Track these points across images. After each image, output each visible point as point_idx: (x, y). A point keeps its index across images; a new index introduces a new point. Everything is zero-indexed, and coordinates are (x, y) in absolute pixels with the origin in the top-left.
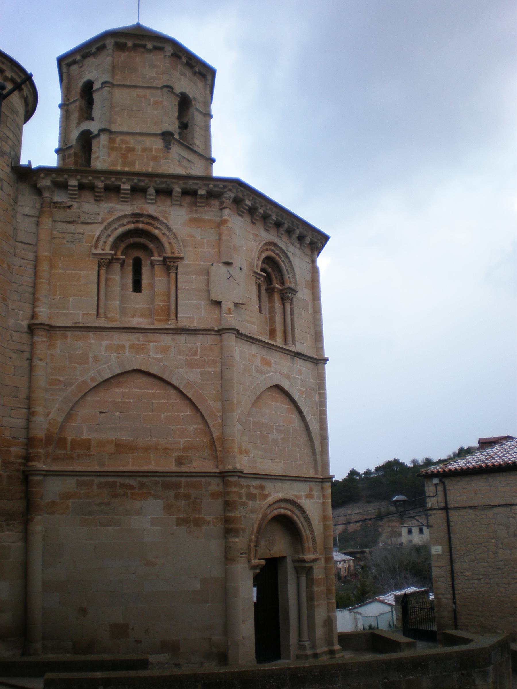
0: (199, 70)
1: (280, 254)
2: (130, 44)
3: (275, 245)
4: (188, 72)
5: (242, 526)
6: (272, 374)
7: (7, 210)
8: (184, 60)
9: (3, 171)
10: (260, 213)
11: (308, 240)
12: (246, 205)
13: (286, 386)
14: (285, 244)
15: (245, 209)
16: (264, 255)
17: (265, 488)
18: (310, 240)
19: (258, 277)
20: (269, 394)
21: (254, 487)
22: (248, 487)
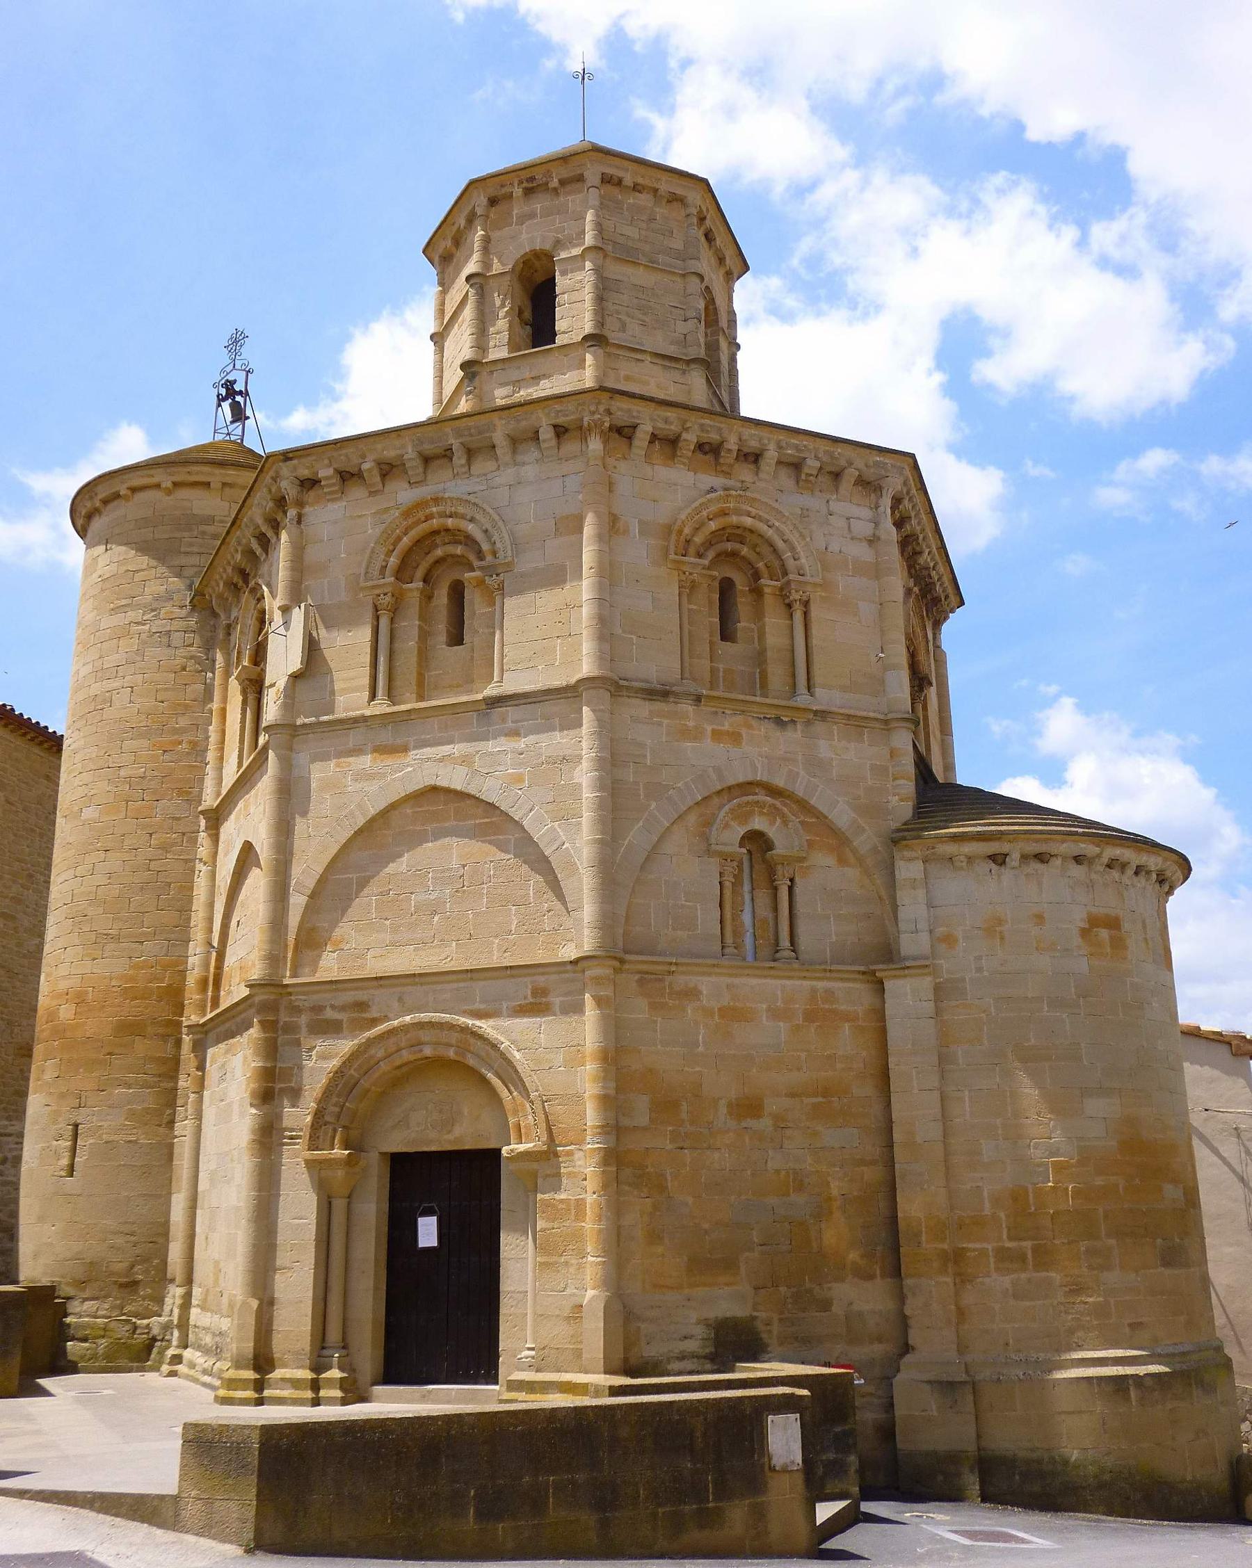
0: (559, 180)
1: (461, 510)
2: (449, 243)
3: (436, 500)
4: (539, 204)
5: (293, 1085)
6: (411, 769)
7: (184, 669)
8: (518, 192)
9: (171, 619)
10: (370, 470)
11: (547, 434)
12: (327, 478)
13: (455, 779)
14: (478, 480)
15: (334, 485)
16: (406, 541)
17: (369, 1006)
18: (551, 429)
19: (377, 592)
20: (417, 812)
21: (333, 1007)
22: (318, 1009)
